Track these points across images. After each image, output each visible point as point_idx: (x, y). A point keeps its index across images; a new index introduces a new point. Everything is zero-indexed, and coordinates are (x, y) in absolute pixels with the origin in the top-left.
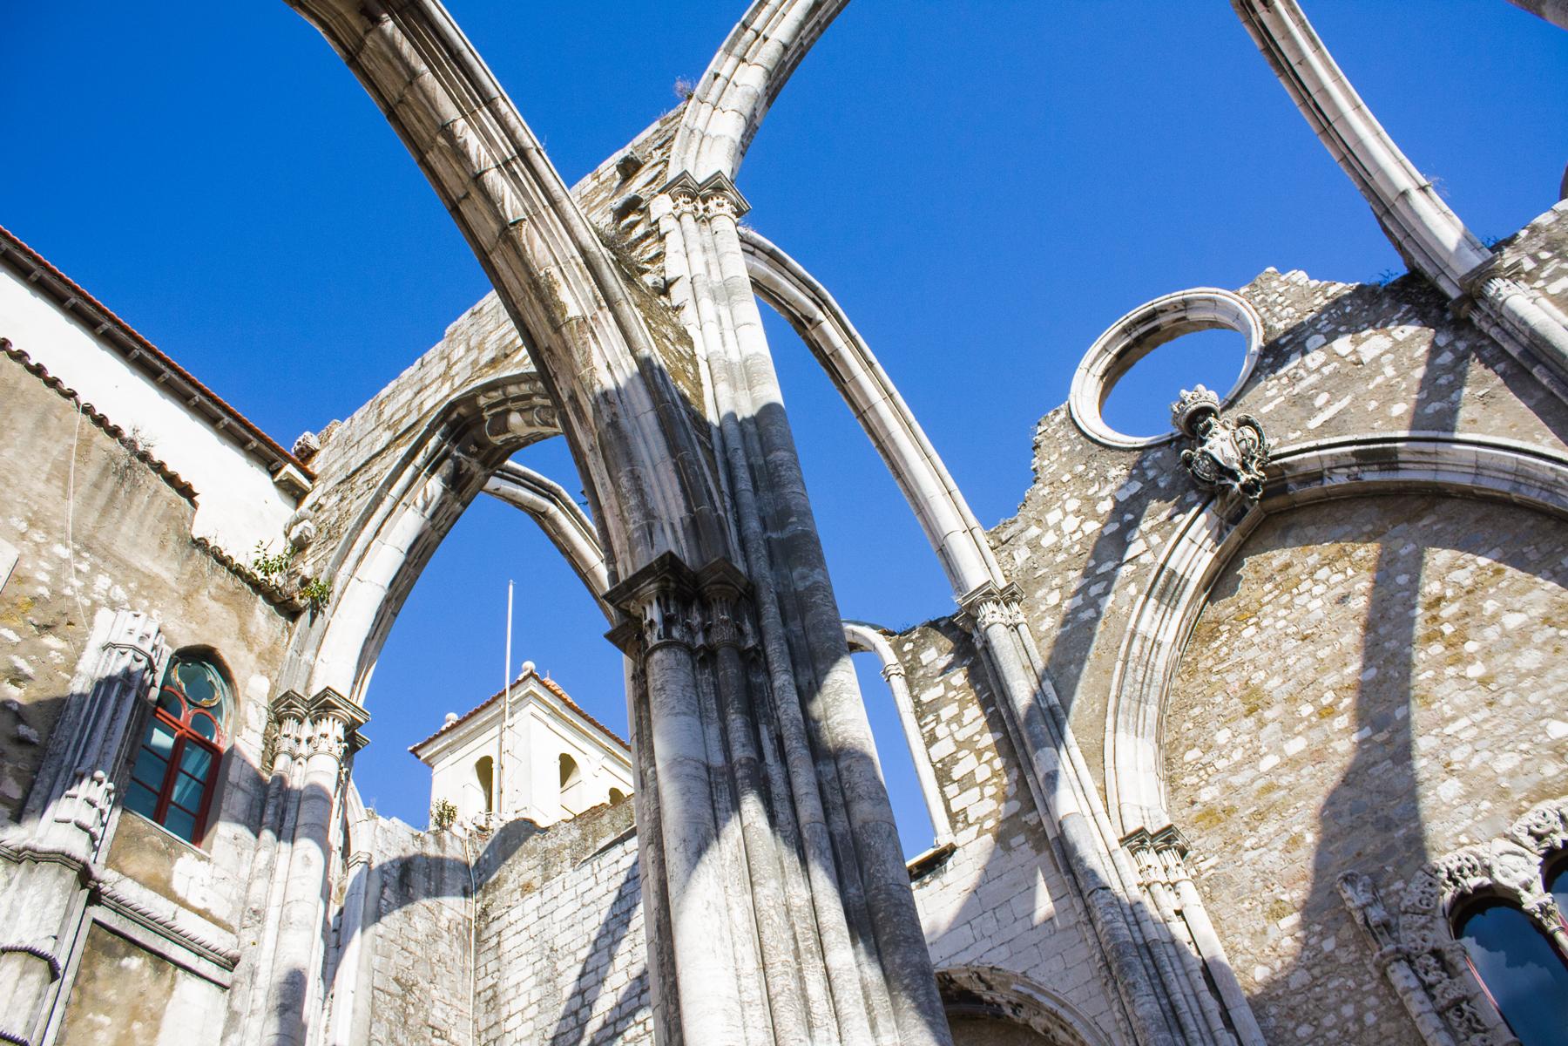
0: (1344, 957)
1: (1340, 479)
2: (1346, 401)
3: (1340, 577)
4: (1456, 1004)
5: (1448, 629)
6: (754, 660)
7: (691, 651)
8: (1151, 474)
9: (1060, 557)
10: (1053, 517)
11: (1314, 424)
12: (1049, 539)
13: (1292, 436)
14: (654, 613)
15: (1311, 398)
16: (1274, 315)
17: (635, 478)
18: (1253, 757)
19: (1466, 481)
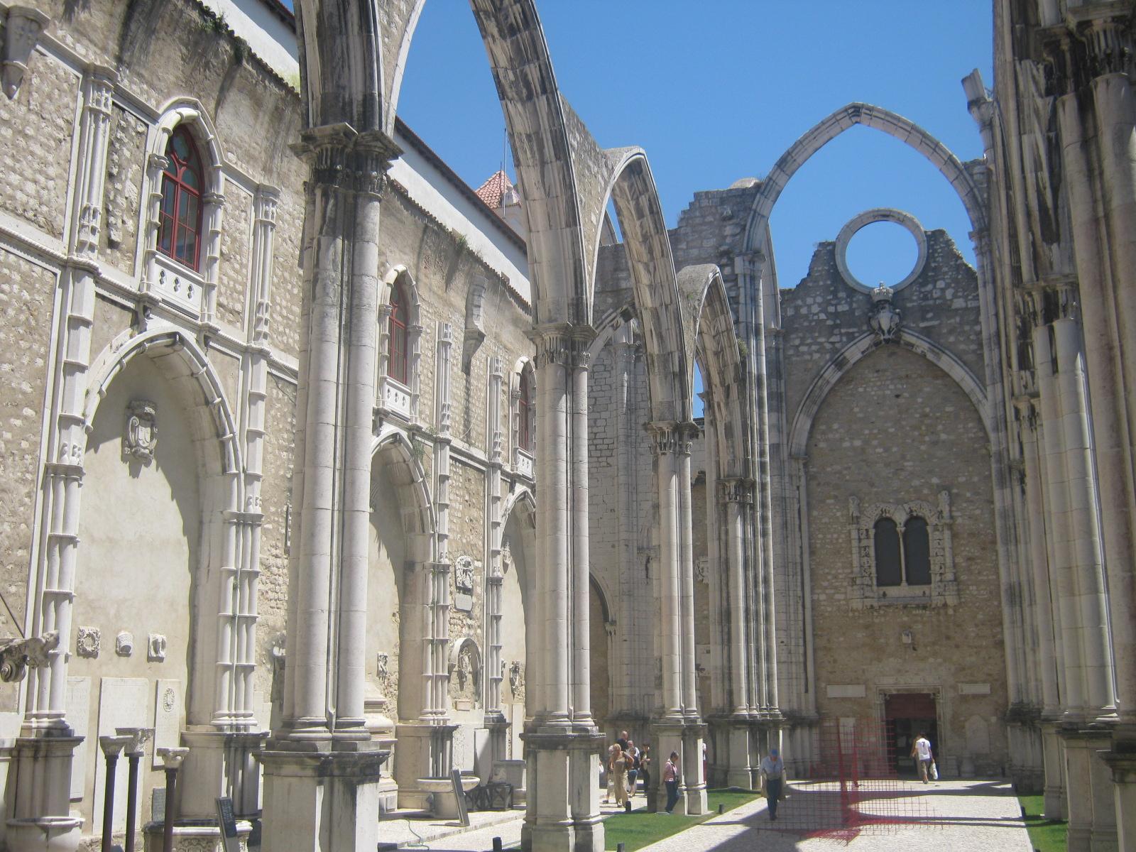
0: (841, 520)
1: (919, 351)
2: (935, 323)
3: (899, 386)
4: (865, 548)
5: (924, 428)
6: (753, 507)
7: (739, 503)
8: (855, 305)
9: (806, 324)
10: (810, 301)
11: (922, 325)
12: (804, 311)
13: (913, 325)
14: (733, 491)
15: (928, 312)
16: (934, 258)
17: (733, 442)
18: (842, 440)
19: (957, 380)
